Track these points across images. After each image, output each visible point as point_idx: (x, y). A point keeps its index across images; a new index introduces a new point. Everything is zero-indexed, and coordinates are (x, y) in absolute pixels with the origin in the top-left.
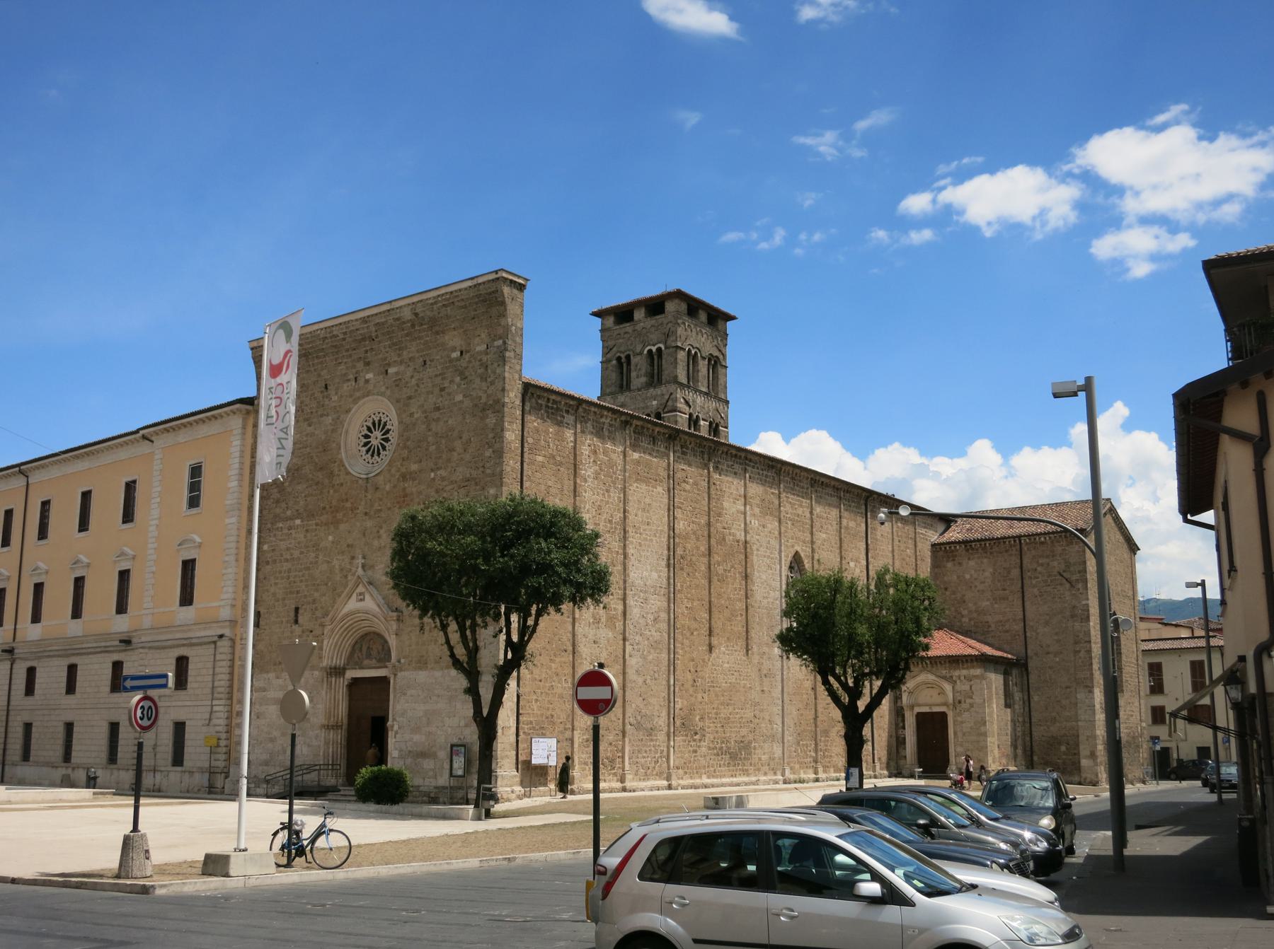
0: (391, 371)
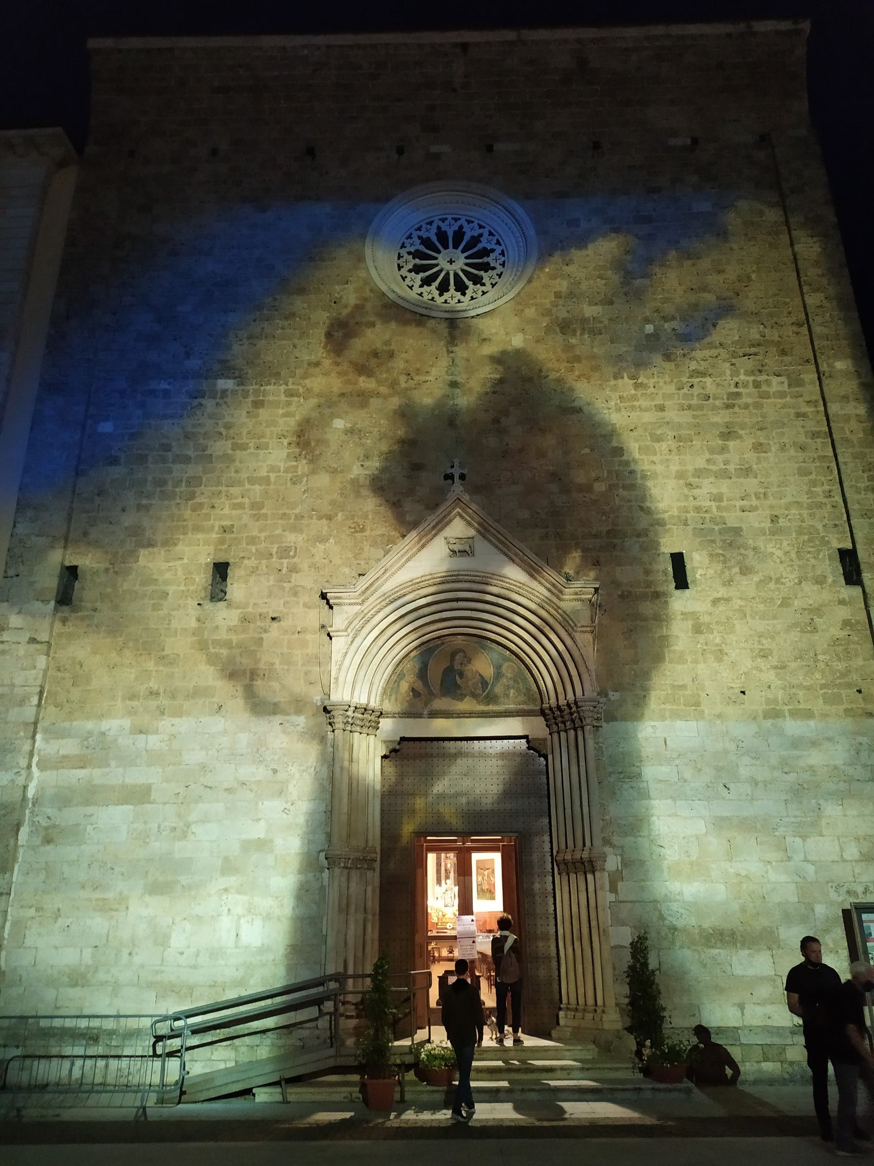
0: (498, 147)
